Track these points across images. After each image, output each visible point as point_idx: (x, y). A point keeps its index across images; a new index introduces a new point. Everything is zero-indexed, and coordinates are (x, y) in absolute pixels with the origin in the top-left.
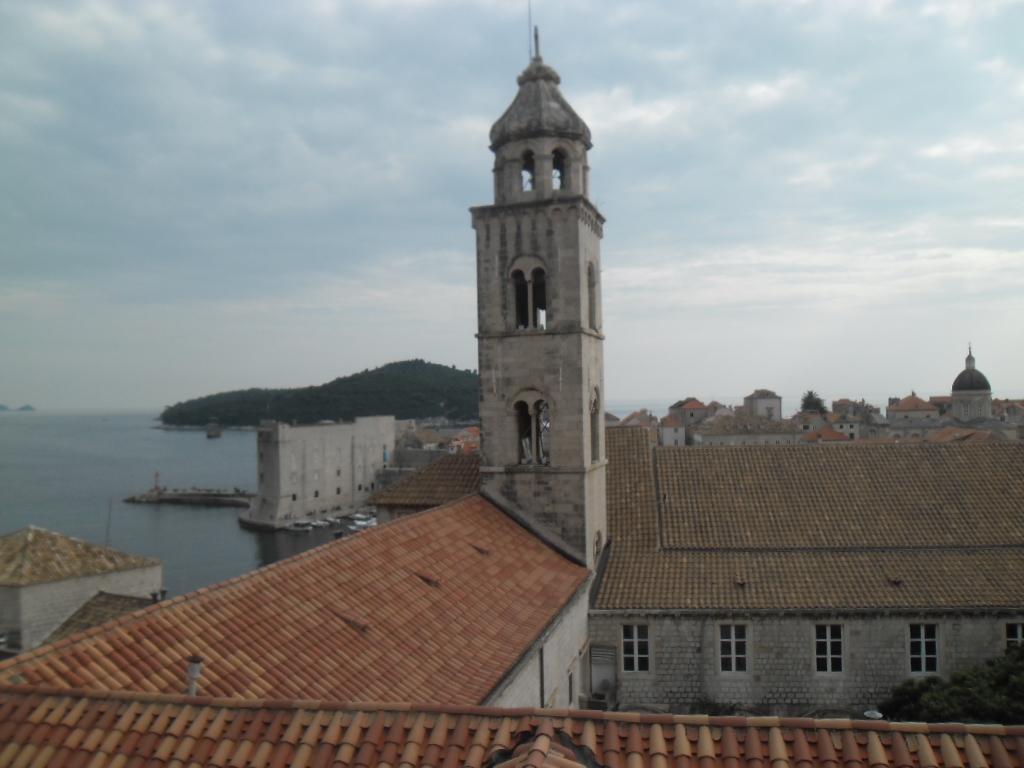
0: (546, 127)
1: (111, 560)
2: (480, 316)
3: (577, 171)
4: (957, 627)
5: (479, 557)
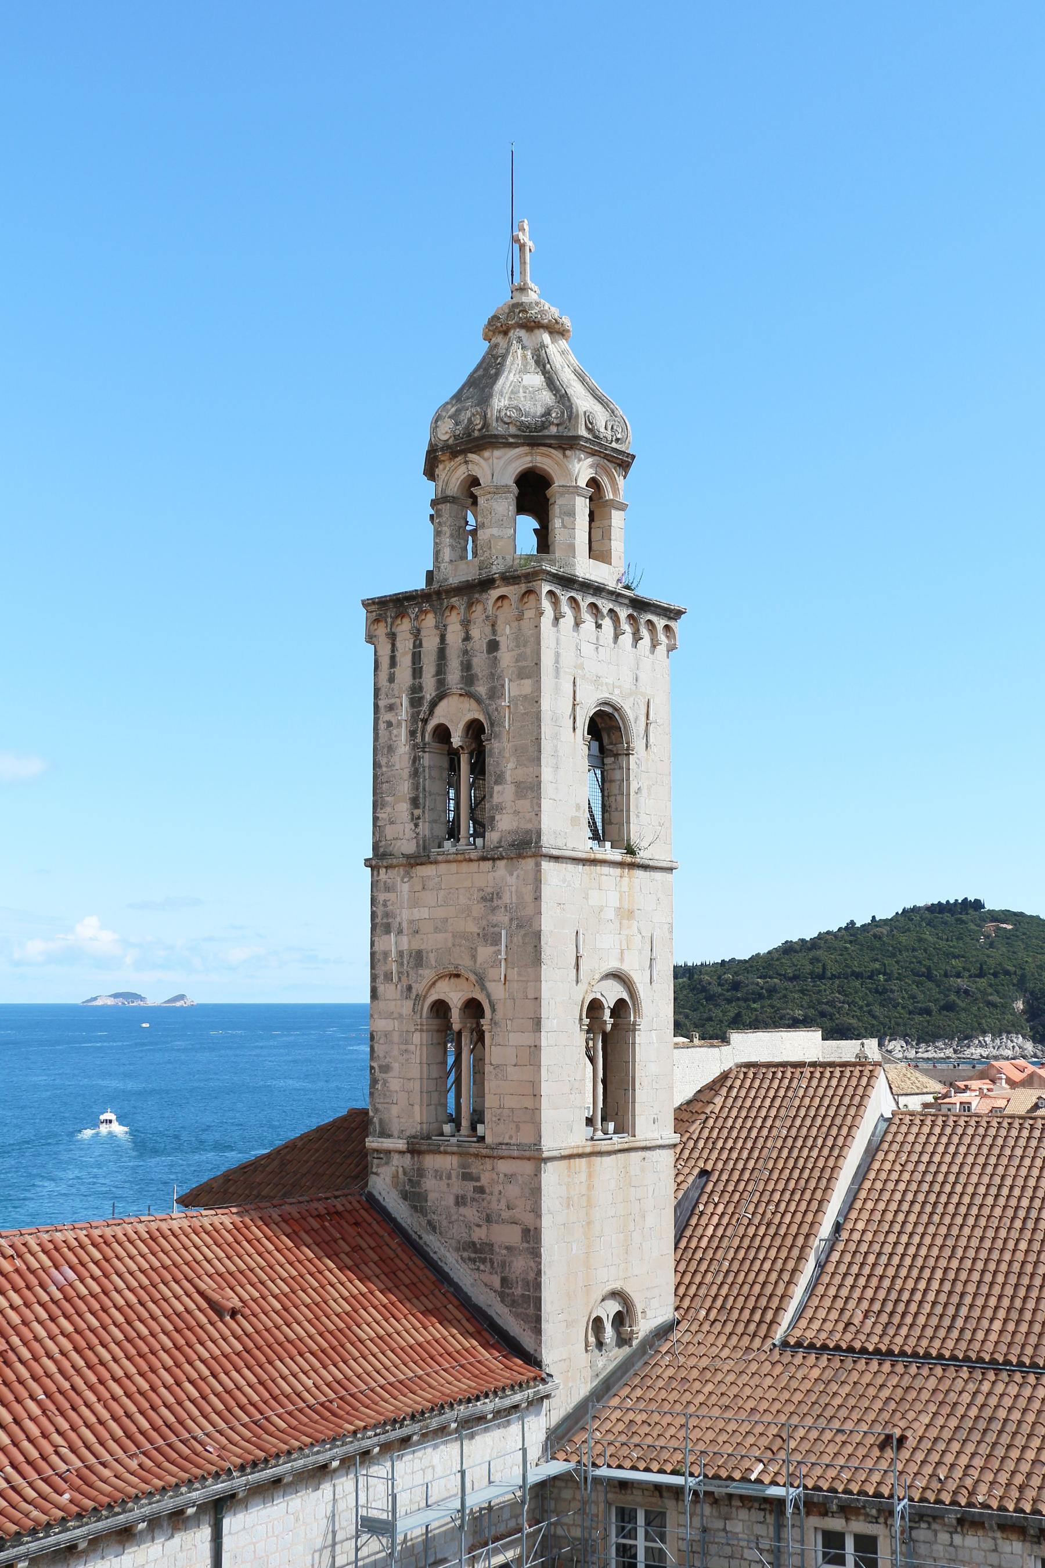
0: (500, 429)
3: (571, 513)
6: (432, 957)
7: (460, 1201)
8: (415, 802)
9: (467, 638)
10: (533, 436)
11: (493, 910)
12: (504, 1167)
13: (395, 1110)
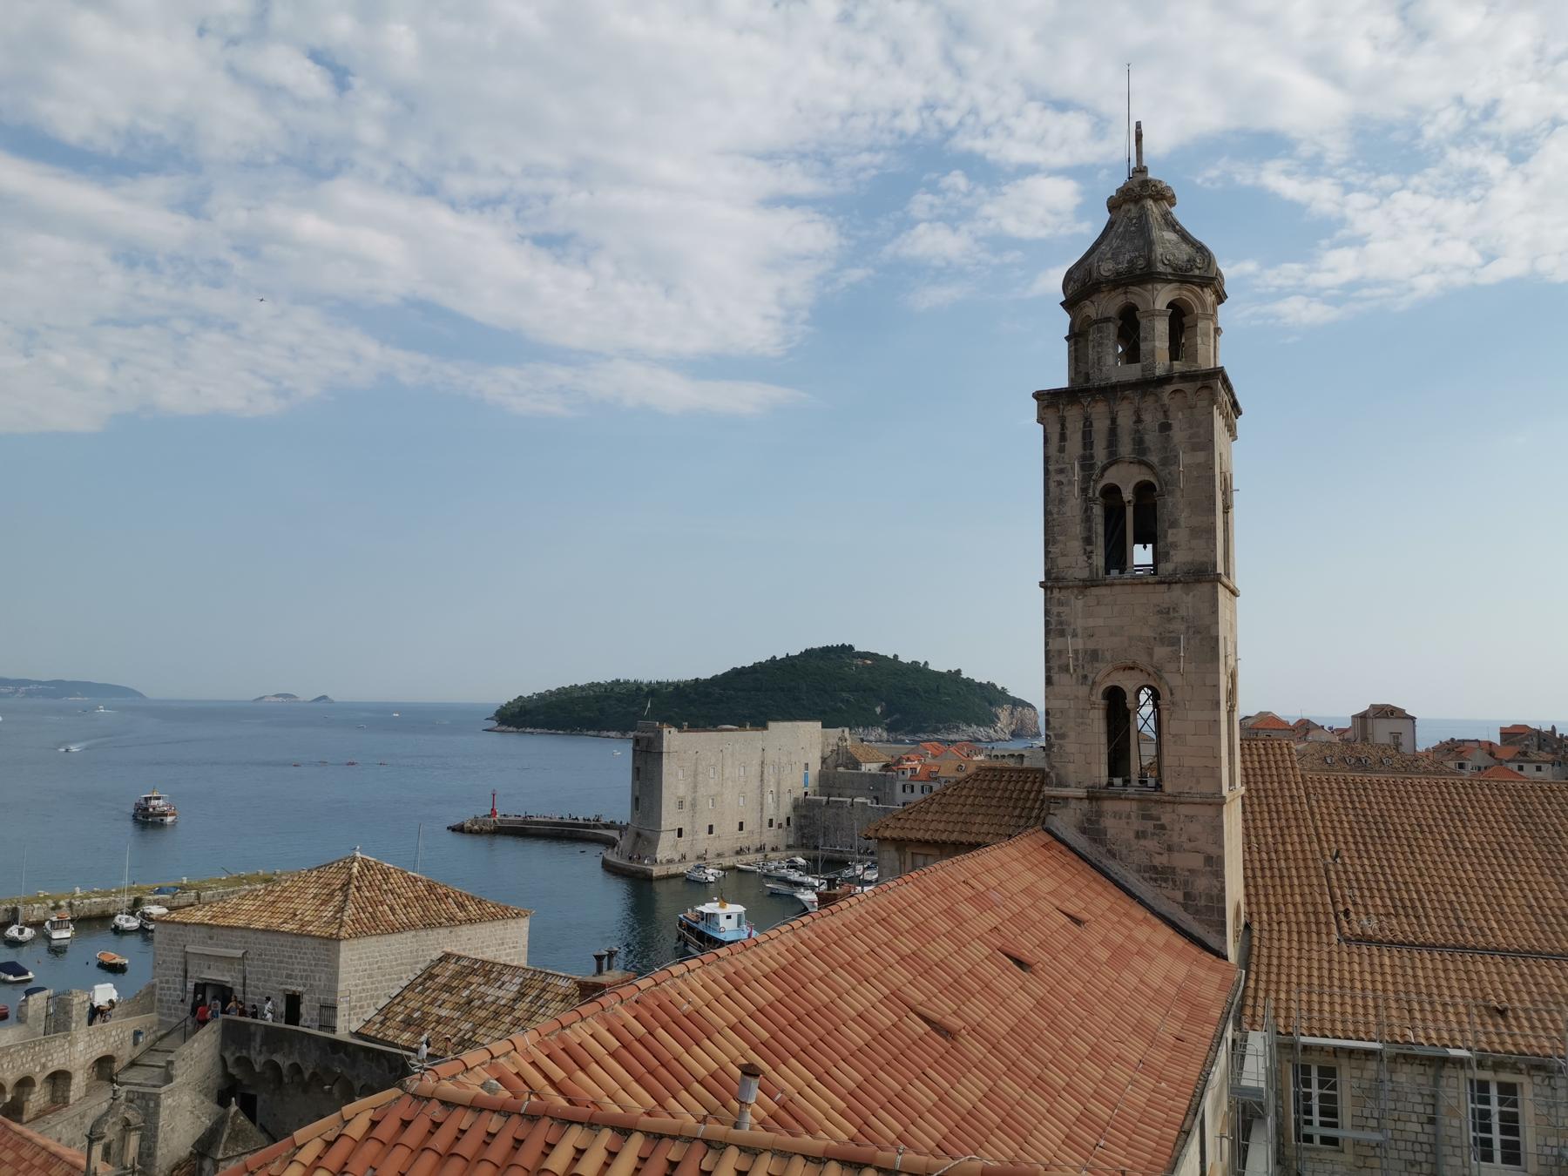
0: (1161, 268)
1: (462, 906)
2: (1047, 553)
3: (1207, 335)
5: (1073, 926)
6: (1108, 655)
9: (1139, 421)
11: (1170, 620)
13: (1071, 767)
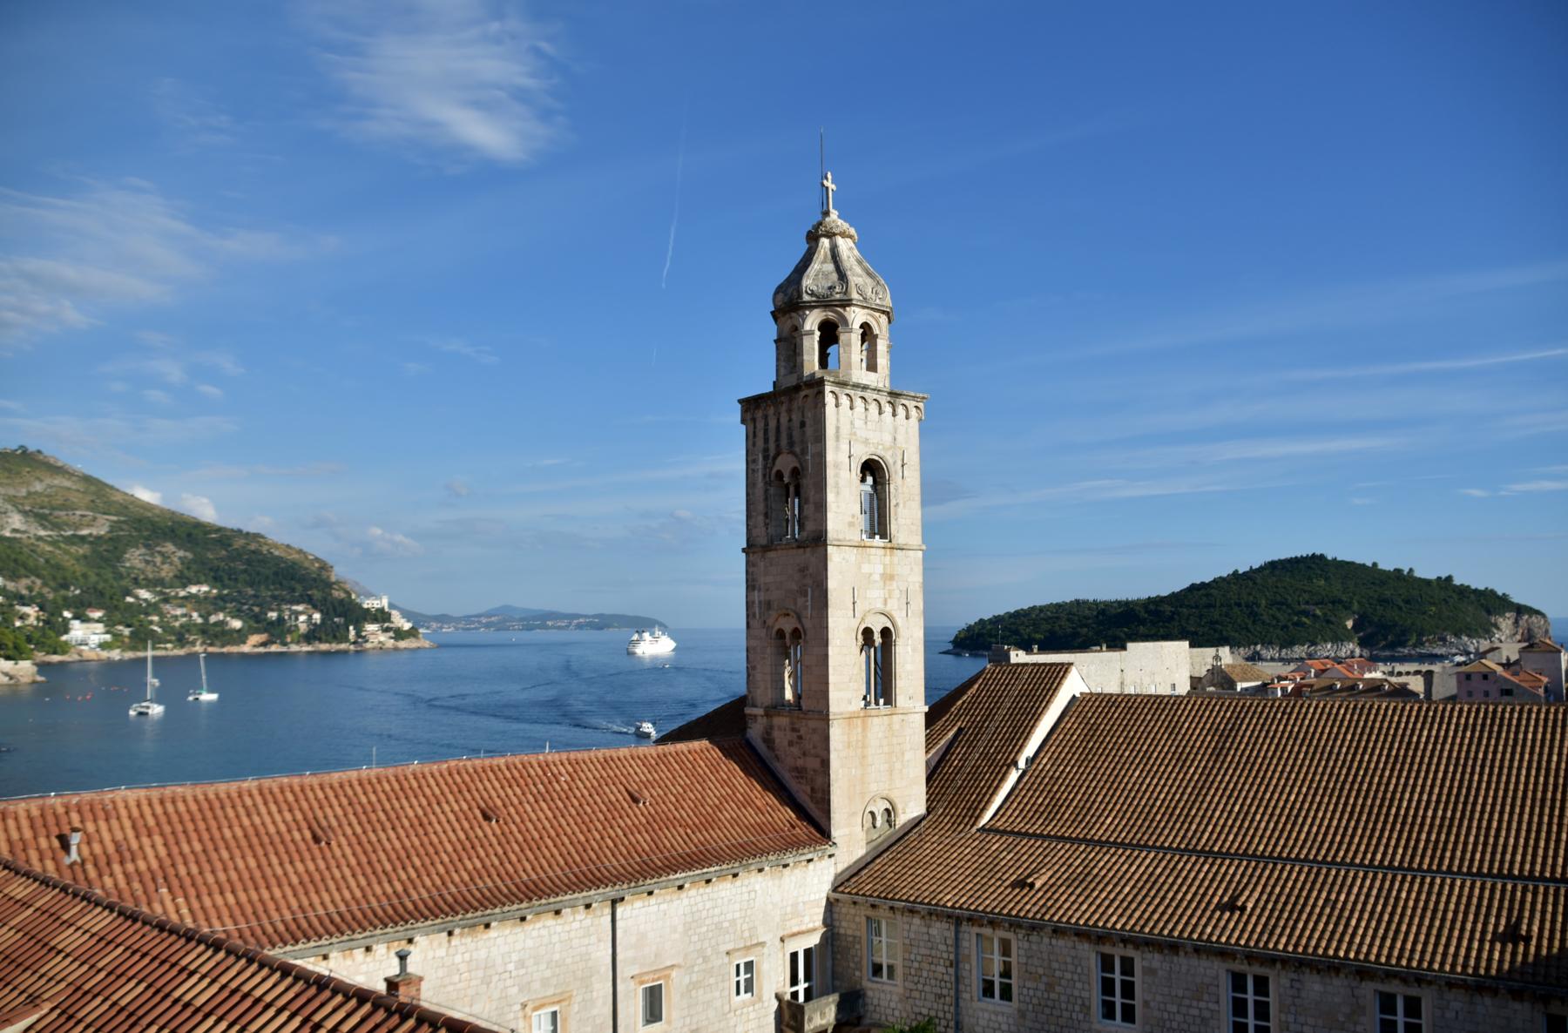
0: (806, 298)
3: (849, 345)
4: (1297, 985)
7: (791, 744)
8: (766, 515)
10: (823, 302)
12: (812, 724)
13: (759, 692)
